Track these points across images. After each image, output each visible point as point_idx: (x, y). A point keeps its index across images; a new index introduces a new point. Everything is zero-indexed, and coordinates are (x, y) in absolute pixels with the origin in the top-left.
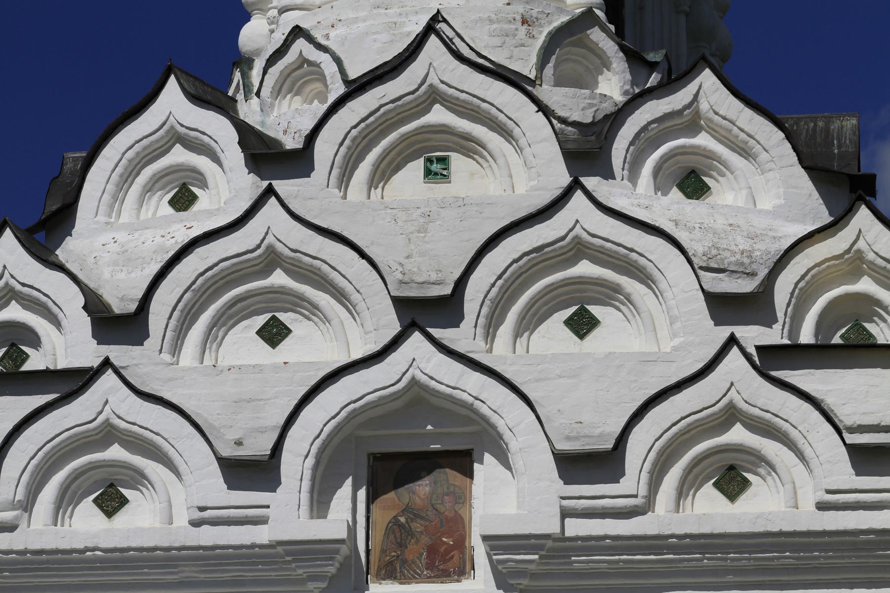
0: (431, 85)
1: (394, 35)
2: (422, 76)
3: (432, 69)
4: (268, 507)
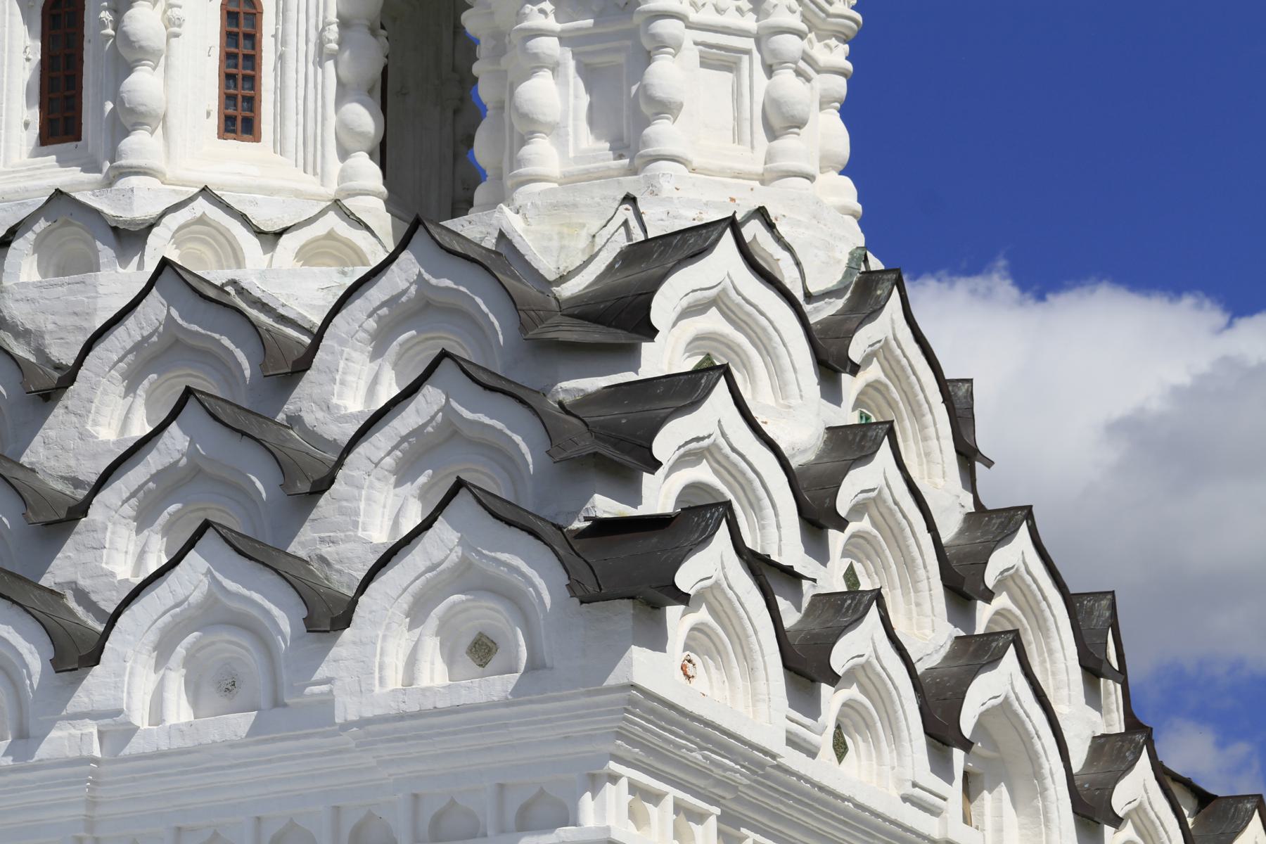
4: (945, 799)
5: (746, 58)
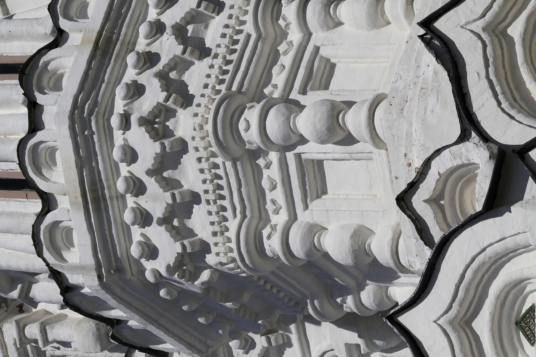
0: (484, 29)
1: (432, 90)
2: (471, 35)
3: (468, 27)
5: (303, 156)
